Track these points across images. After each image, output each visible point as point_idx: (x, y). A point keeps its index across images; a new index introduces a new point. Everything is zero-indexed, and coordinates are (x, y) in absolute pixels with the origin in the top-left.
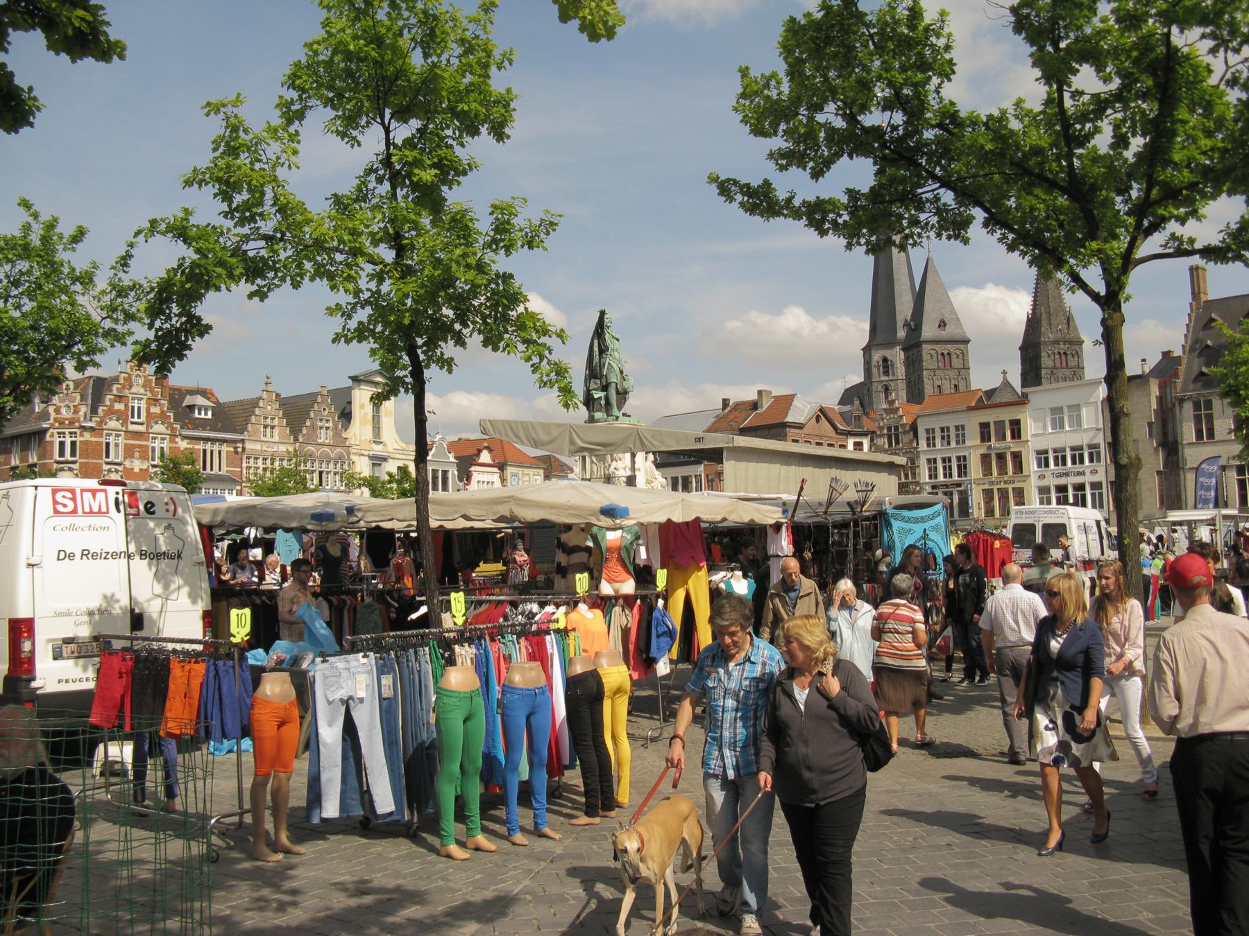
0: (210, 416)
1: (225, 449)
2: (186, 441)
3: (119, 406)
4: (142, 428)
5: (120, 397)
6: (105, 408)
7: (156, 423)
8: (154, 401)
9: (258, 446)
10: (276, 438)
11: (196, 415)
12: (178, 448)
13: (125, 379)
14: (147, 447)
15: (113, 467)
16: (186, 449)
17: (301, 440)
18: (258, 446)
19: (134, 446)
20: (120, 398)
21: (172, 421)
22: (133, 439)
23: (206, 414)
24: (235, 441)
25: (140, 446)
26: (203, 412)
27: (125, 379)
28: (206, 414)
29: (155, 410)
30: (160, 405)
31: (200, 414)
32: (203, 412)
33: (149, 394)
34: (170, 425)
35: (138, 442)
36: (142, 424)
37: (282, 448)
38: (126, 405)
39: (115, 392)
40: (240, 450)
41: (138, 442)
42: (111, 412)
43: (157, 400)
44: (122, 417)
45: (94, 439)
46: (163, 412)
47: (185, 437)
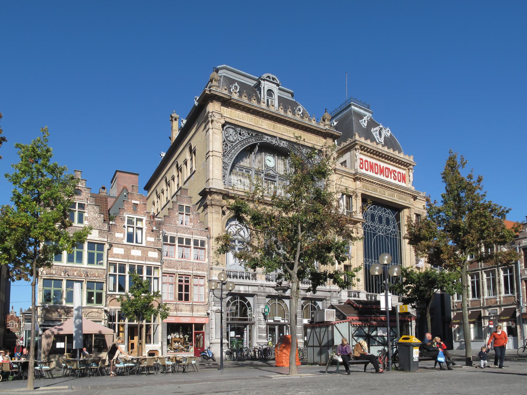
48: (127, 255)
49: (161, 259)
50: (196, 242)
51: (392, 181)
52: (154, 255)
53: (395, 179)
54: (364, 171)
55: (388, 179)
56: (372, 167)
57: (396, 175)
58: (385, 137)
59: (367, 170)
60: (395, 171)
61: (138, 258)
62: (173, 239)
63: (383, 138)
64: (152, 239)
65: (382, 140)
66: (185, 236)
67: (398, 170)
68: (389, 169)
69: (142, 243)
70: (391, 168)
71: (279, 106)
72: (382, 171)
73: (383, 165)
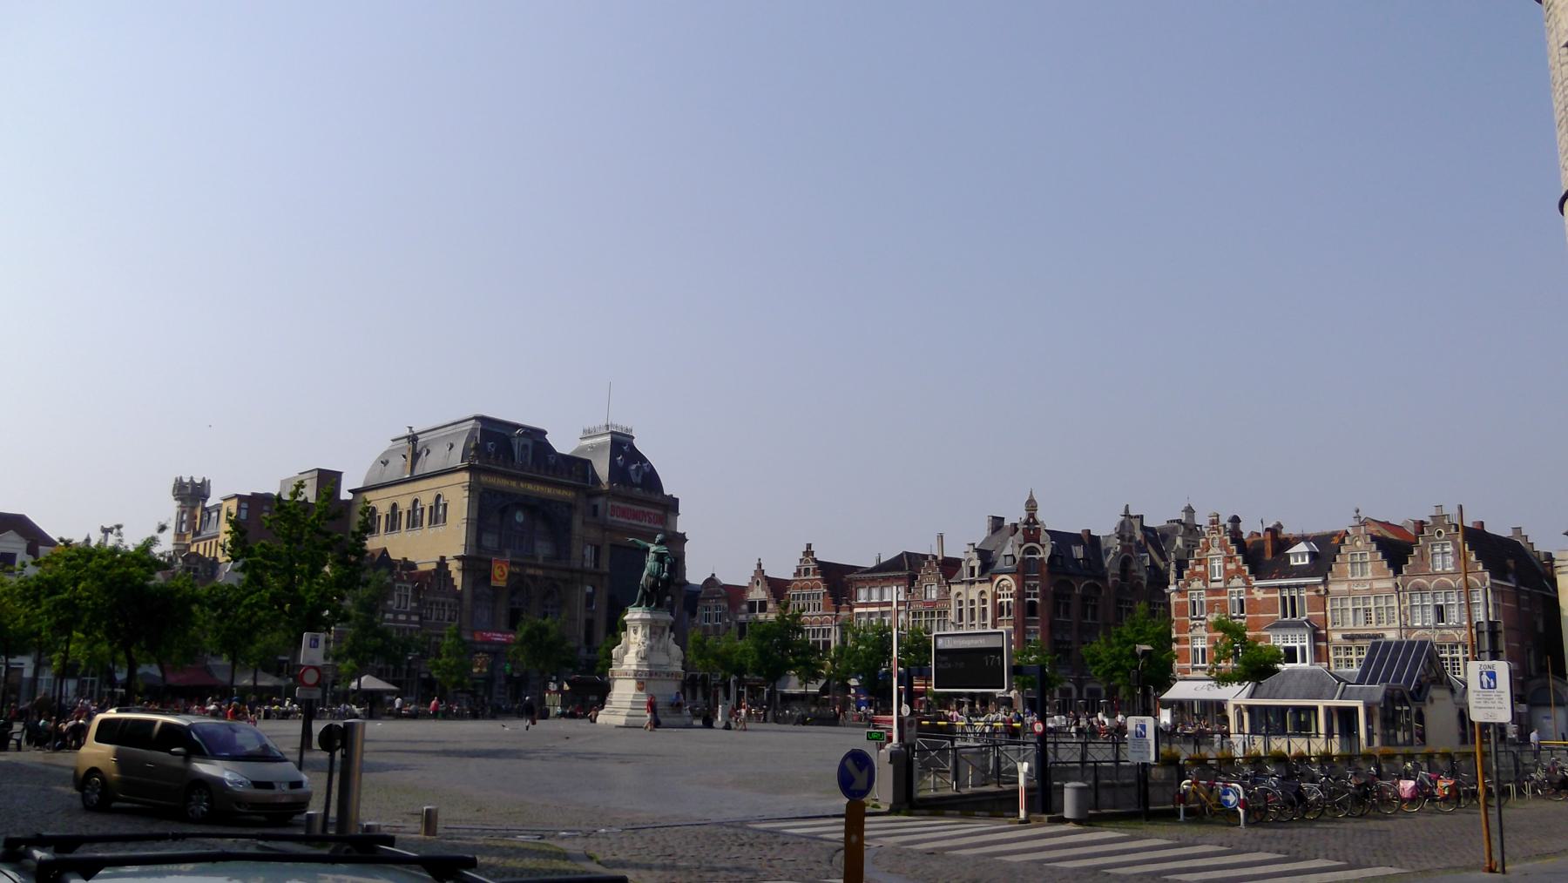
0: (1307, 562)
1: (1305, 594)
2: (1262, 591)
3: (1199, 569)
4: (1221, 585)
5: (1200, 560)
6: (1188, 572)
7: (1233, 578)
8: (1230, 559)
9: (1344, 587)
10: (1370, 576)
11: (1292, 562)
12: (1255, 599)
13: (1203, 544)
14: (1226, 601)
15: (1198, 623)
16: (1263, 599)
17: (1404, 572)
18: (1344, 587)
19: (1214, 602)
20: (1199, 562)
21: (1247, 573)
22: (1213, 596)
23: (1304, 560)
24: (1316, 585)
25: (1219, 601)
26: (1300, 559)
27: (1203, 544)
28: (1304, 560)
29: (1231, 566)
30: (1235, 560)
31: (1297, 561)
32: (1300, 559)
33: (1224, 552)
34: (1247, 581)
35: (1218, 598)
36: (1220, 581)
37: (1377, 585)
38: (1206, 566)
39: (1196, 557)
40: (1323, 593)
41: (1218, 598)
42: (1194, 574)
43: (1231, 557)
44: (1204, 577)
45: (1180, 600)
46: (1238, 567)
47: (1261, 587)
48: (395, 620)
49: (420, 622)
50: (450, 606)
51: (647, 524)
52: (415, 618)
53: (649, 522)
54: (615, 518)
55: (643, 523)
56: (624, 513)
57: (652, 517)
58: (643, 477)
59: (617, 516)
60: (651, 514)
61: (403, 622)
62: (431, 604)
63: (640, 477)
64: (414, 605)
65: (639, 480)
66: (442, 599)
67: (652, 511)
68: (643, 512)
69: (406, 608)
70: (646, 510)
71: (532, 463)
72: (636, 516)
73: (637, 508)
